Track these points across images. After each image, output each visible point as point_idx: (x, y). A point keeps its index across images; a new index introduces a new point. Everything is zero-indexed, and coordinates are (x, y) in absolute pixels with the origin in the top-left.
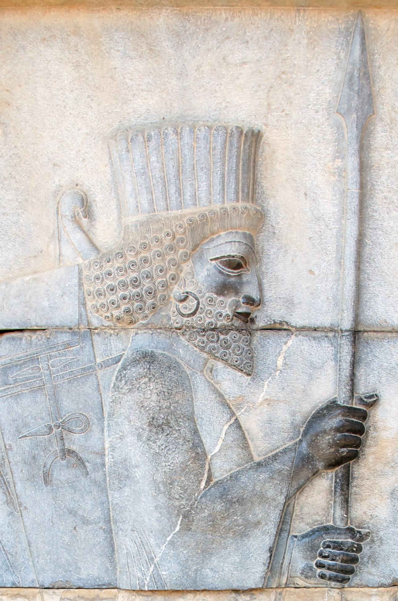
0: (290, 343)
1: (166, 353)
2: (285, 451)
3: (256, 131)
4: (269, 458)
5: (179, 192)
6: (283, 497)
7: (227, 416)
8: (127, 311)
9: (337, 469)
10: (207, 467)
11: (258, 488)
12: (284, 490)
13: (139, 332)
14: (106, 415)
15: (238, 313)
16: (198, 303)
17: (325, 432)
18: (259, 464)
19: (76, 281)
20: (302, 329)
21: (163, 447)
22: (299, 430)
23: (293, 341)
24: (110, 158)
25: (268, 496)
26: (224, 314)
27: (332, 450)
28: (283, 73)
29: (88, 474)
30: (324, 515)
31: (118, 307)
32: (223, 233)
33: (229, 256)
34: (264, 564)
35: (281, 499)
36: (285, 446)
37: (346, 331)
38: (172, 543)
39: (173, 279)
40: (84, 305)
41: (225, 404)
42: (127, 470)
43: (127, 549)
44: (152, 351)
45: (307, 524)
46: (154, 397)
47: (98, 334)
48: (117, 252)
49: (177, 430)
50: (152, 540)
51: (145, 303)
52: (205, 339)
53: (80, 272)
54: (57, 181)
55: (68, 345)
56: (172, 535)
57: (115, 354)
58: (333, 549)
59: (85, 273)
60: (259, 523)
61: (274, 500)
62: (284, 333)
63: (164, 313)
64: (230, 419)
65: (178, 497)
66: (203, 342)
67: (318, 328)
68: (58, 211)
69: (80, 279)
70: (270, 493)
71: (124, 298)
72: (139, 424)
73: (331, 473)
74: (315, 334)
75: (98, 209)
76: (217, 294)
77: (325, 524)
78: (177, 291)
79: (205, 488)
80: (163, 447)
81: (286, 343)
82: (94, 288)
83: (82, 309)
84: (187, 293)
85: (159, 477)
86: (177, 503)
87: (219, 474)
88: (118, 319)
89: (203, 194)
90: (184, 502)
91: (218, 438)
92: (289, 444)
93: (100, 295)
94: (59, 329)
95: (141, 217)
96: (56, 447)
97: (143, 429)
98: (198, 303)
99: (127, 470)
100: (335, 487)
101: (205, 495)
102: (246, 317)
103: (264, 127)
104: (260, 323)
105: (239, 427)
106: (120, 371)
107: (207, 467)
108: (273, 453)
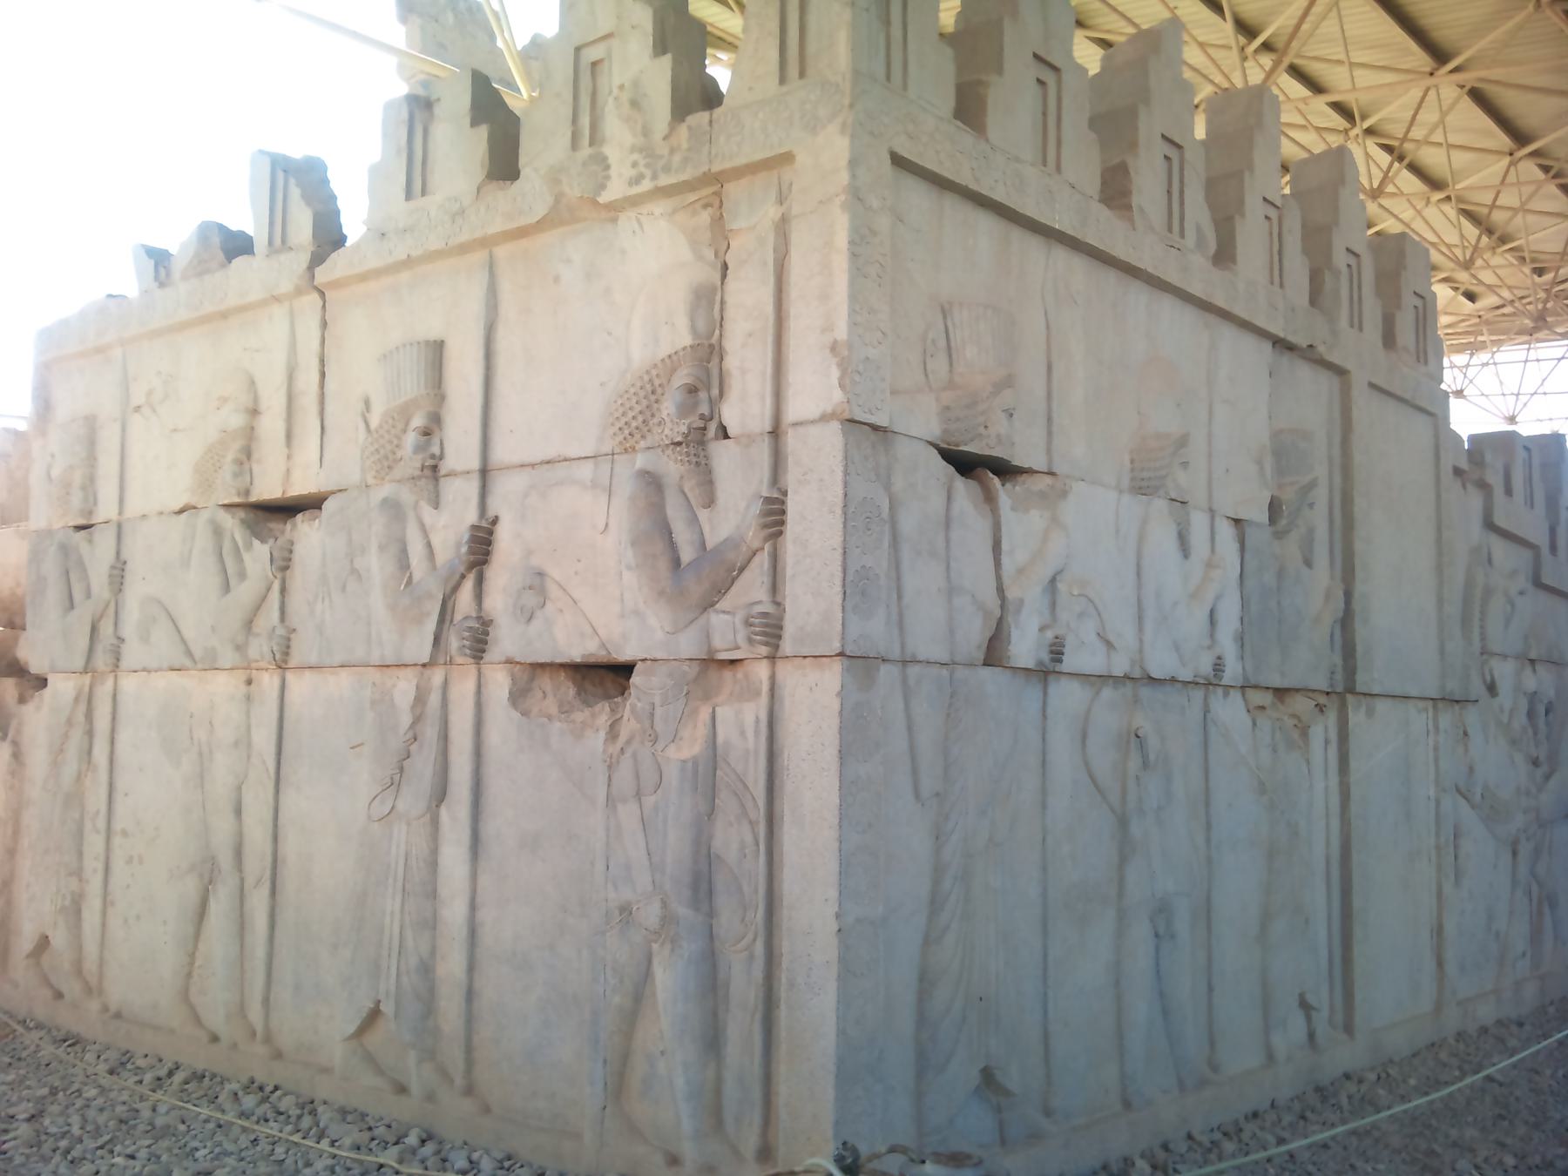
102: (435, 468)
104: (443, 471)
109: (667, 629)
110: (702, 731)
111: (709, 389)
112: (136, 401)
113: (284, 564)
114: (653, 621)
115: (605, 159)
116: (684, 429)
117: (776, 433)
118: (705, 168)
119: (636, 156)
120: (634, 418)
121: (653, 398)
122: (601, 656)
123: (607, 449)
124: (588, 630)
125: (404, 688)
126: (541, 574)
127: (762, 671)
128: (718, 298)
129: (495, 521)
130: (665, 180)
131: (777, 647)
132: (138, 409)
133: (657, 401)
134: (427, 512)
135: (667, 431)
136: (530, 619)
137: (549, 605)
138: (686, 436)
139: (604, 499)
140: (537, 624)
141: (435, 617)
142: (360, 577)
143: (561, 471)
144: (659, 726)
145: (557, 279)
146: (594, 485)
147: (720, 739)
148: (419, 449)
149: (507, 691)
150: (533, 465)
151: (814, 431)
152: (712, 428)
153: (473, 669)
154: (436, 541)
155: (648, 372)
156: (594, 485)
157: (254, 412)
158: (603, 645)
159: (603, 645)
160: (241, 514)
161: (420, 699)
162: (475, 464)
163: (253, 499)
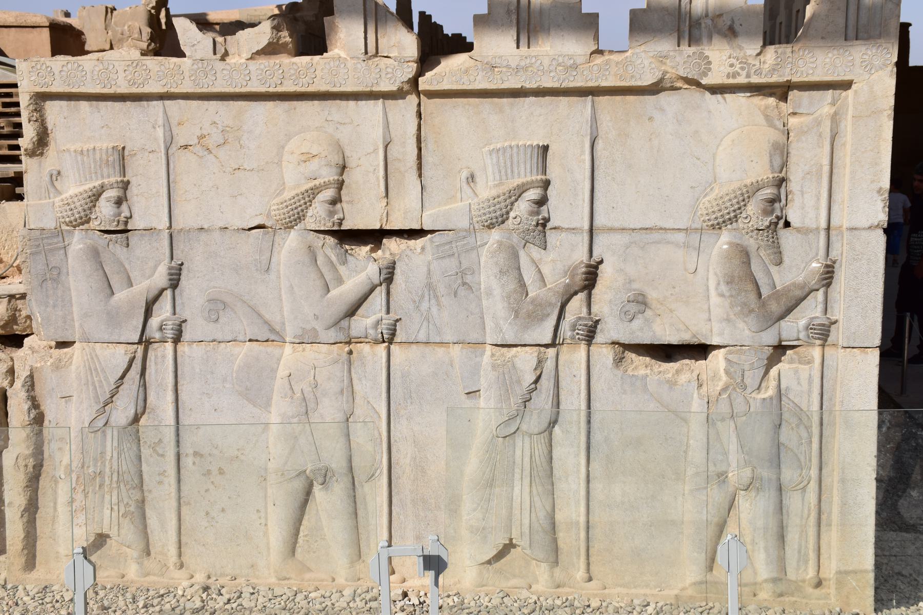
5: (512, 172)
7: (534, 268)
17: (577, 274)
23: (563, 234)
38: (510, 323)
41: (533, 261)
46: (502, 260)
59: (472, 206)
74: (573, 231)
85: (504, 294)
86: (512, 306)
95: (496, 183)
96: (460, 281)
109: (753, 330)
110: (773, 384)
111: (780, 201)
113: (389, 276)
114: (741, 325)
115: (707, 57)
116: (767, 223)
117: (828, 229)
118: (789, 79)
119: (733, 61)
120: (729, 213)
121: (742, 203)
122: (695, 341)
124: (681, 326)
125: (526, 359)
127: (816, 352)
128: (786, 150)
130: (755, 80)
131: (826, 340)
132: (186, 147)
133: (745, 205)
134: (535, 252)
135: (751, 223)
136: (631, 320)
137: (649, 313)
138: (768, 227)
139: (695, 254)
140: (637, 323)
141: (554, 316)
142: (470, 288)
143: (656, 236)
144: (748, 381)
145: (651, 119)
146: (687, 246)
147: (783, 386)
150: (633, 230)
151: (864, 233)
152: (781, 223)
153: (583, 347)
154: (546, 270)
155: (740, 189)
158: (694, 336)
159: (694, 336)
161: (540, 362)
162: (586, 226)
163: (346, 226)
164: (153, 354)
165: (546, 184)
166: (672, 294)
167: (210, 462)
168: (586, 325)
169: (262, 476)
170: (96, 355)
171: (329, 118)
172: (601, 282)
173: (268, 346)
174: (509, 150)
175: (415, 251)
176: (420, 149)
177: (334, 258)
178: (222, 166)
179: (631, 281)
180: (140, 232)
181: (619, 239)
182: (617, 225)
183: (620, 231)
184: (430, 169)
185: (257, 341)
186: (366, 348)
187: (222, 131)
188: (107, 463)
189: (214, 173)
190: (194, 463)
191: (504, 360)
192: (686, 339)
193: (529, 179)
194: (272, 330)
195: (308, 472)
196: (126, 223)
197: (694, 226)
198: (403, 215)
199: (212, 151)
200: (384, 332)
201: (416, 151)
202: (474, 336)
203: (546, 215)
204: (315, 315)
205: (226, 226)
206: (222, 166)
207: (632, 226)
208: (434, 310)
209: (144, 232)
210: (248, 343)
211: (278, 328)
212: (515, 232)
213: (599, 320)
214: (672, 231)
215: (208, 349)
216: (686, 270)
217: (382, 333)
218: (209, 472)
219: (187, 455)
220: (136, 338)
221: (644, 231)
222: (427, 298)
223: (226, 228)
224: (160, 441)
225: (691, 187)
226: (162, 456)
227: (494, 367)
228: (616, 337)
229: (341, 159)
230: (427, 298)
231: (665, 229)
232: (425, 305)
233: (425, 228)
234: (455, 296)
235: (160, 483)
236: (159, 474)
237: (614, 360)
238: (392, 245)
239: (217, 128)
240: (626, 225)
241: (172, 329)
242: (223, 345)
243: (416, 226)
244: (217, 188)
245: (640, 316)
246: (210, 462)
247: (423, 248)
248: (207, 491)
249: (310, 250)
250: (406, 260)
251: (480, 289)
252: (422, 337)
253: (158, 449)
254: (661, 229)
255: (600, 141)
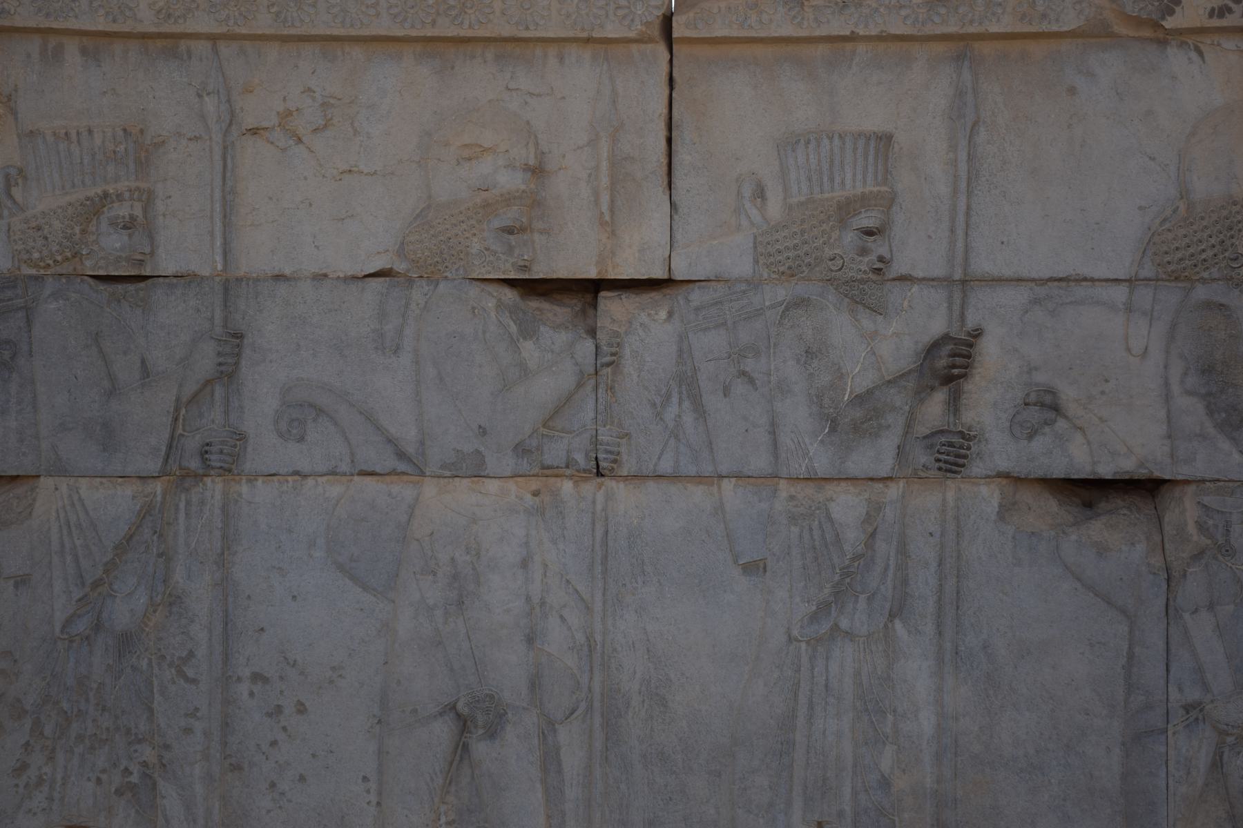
0: (914, 290)
1: (819, 298)
2: (910, 372)
3: (888, 134)
4: (897, 377)
6: (908, 407)
8: (790, 268)
9: (951, 385)
10: (849, 384)
11: (889, 400)
12: (909, 402)
13: (799, 283)
14: (772, 345)
15: (875, 269)
16: (844, 262)
18: (889, 382)
19: (751, 245)
20: (924, 279)
21: (816, 369)
22: (920, 357)
23: (915, 288)
24: (779, 154)
25: (897, 406)
26: (863, 270)
27: (946, 371)
28: (909, 90)
29: (757, 389)
30: (941, 421)
31: (784, 265)
32: (863, 210)
33: (868, 227)
34: (894, 458)
35: (907, 408)
36: (909, 368)
37: (957, 281)
38: (822, 441)
39: (825, 244)
40: (758, 262)
42: (788, 386)
43: (787, 446)
44: (809, 298)
45: (927, 428)
47: (767, 284)
48: (784, 224)
49: (826, 356)
50: (807, 440)
51: (804, 262)
52: (848, 288)
53: (755, 237)
54: (738, 170)
55: (744, 292)
56: (822, 436)
57: (780, 299)
58: (948, 447)
59: (759, 239)
60: (889, 426)
61: (901, 409)
62: (909, 283)
63: (818, 269)
64: (867, 347)
65: (826, 406)
66: (847, 291)
67: (935, 278)
68: (738, 193)
69: (755, 243)
70: (898, 404)
71: (789, 259)
72: (799, 352)
73: (945, 389)
74: (931, 283)
75: (769, 194)
76: (858, 255)
77: (941, 428)
78: (828, 252)
79: (848, 399)
80: (816, 369)
81: (910, 290)
82: (766, 250)
83: (756, 266)
84: (835, 254)
86: (826, 411)
87: (858, 391)
88: (783, 273)
89: (848, 182)
90: (831, 410)
91: (858, 362)
92: (912, 366)
93: (771, 255)
94: (739, 280)
95: (803, 199)
97: (801, 355)
98: (844, 262)
99: (788, 386)
100: (949, 400)
101: (847, 405)
103: (894, 130)
105: (874, 353)
106: (783, 312)
107: (849, 384)
108: (901, 373)
112: (250, 122)
122: (1142, 473)
123: (1147, 271)
126: (1052, 392)
129: (977, 333)
132: (254, 131)
136: (1030, 437)
142: (752, 381)
145: (1072, 91)
148: (863, 251)
149: (996, 505)
156: (1129, 309)
157: (538, 171)
159: (1142, 465)
160: (509, 295)
163: (539, 272)
164: (183, 498)
165: (890, 201)
166: (1103, 393)
167: (281, 692)
168: (951, 445)
169: (374, 716)
170: (80, 499)
171: (512, 85)
172: (980, 370)
173: (392, 483)
174: (826, 141)
175: (656, 317)
176: (669, 141)
177: (513, 328)
178: (321, 165)
179: (1031, 369)
180: (167, 280)
181: (1014, 297)
182: (1007, 272)
183: (1015, 283)
184: (686, 175)
185: (372, 474)
186: (567, 486)
187: (323, 105)
188: (91, 694)
189: (306, 178)
190: (252, 694)
191: (810, 507)
192: (1128, 469)
193: (859, 190)
194: (401, 455)
195: (460, 706)
196: (141, 262)
197: (1145, 273)
198: (637, 255)
199: (304, 139)
200: (601, 456)
201: (663, 143)
202: (760, 462)
203: (888, 256)
204: (480, 427)
205: (324, 271)
206: (321, 165)
207: (1034, 275)
208: (688, 419)
209: (175, 280)
210: (356, 478)
211: (411, 450)
212: (832, 285)
213: (975, 437)
214: (1104, 283)
215: (285, 488)
216: (1129, 350)
217: (596, 458)
218: (279, 709)
219: (239, 679)
220: (154, 466)
221: (1056, 283)
222: (675, 399)
223: (325, 275)
224: (191, 654)
225: (1140, 208)
226: (194, 681)
227: (793, 519)
228: (1003, 465)
229: (532, 156)
230: (675, 399)
231: (1092, 280)
232: (671, 412)
233: (678, 276)
234: (725, 396)
235: (188, 731)
236: (186, 715)
237: (1001, 506)
238: (613, 307)
239: (314, 99)
240: (1025, 273)
241: (221, 452)
242: (310, 482)
243: (659, 273)
244: (311, 205)
245: (1047, 429)
246: (281, 692)
247: (670, 314)
248: (274, 743)
249: (474, 312)
250: (641, 332)
251: (770, 382)
252: (666, 466)
253: (185, 669)
254: (1085, 279)
255: (982, 129)
